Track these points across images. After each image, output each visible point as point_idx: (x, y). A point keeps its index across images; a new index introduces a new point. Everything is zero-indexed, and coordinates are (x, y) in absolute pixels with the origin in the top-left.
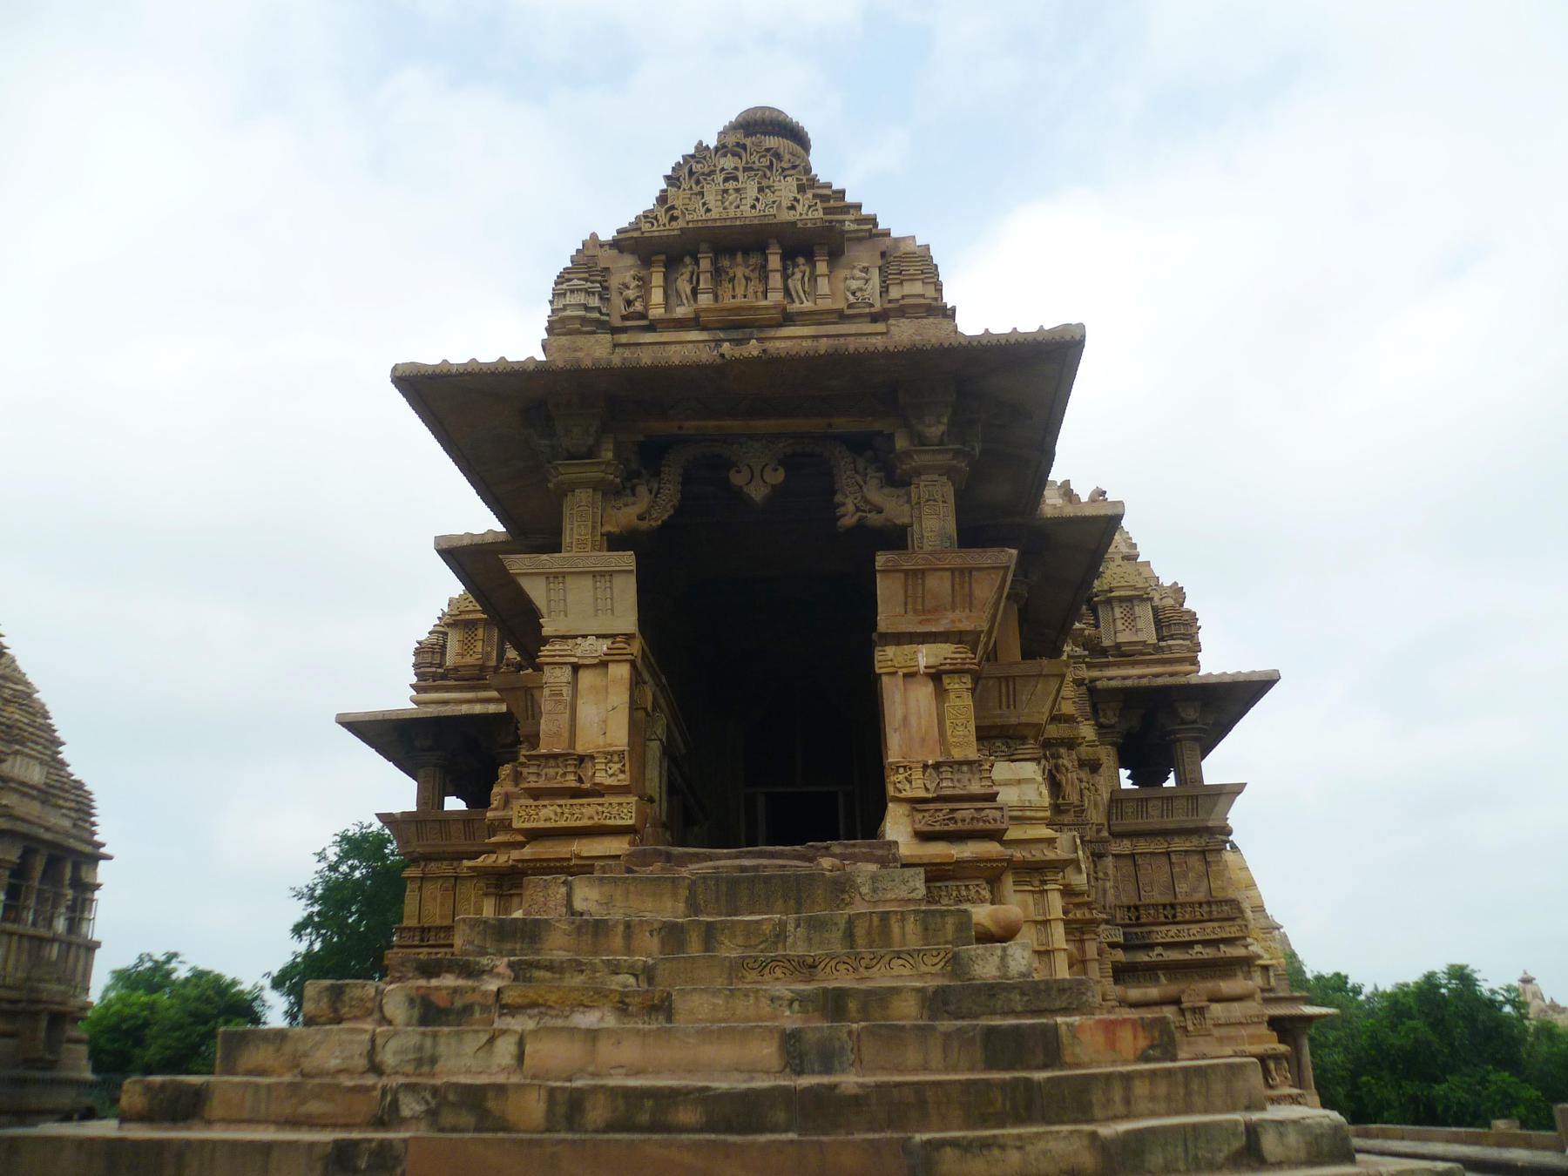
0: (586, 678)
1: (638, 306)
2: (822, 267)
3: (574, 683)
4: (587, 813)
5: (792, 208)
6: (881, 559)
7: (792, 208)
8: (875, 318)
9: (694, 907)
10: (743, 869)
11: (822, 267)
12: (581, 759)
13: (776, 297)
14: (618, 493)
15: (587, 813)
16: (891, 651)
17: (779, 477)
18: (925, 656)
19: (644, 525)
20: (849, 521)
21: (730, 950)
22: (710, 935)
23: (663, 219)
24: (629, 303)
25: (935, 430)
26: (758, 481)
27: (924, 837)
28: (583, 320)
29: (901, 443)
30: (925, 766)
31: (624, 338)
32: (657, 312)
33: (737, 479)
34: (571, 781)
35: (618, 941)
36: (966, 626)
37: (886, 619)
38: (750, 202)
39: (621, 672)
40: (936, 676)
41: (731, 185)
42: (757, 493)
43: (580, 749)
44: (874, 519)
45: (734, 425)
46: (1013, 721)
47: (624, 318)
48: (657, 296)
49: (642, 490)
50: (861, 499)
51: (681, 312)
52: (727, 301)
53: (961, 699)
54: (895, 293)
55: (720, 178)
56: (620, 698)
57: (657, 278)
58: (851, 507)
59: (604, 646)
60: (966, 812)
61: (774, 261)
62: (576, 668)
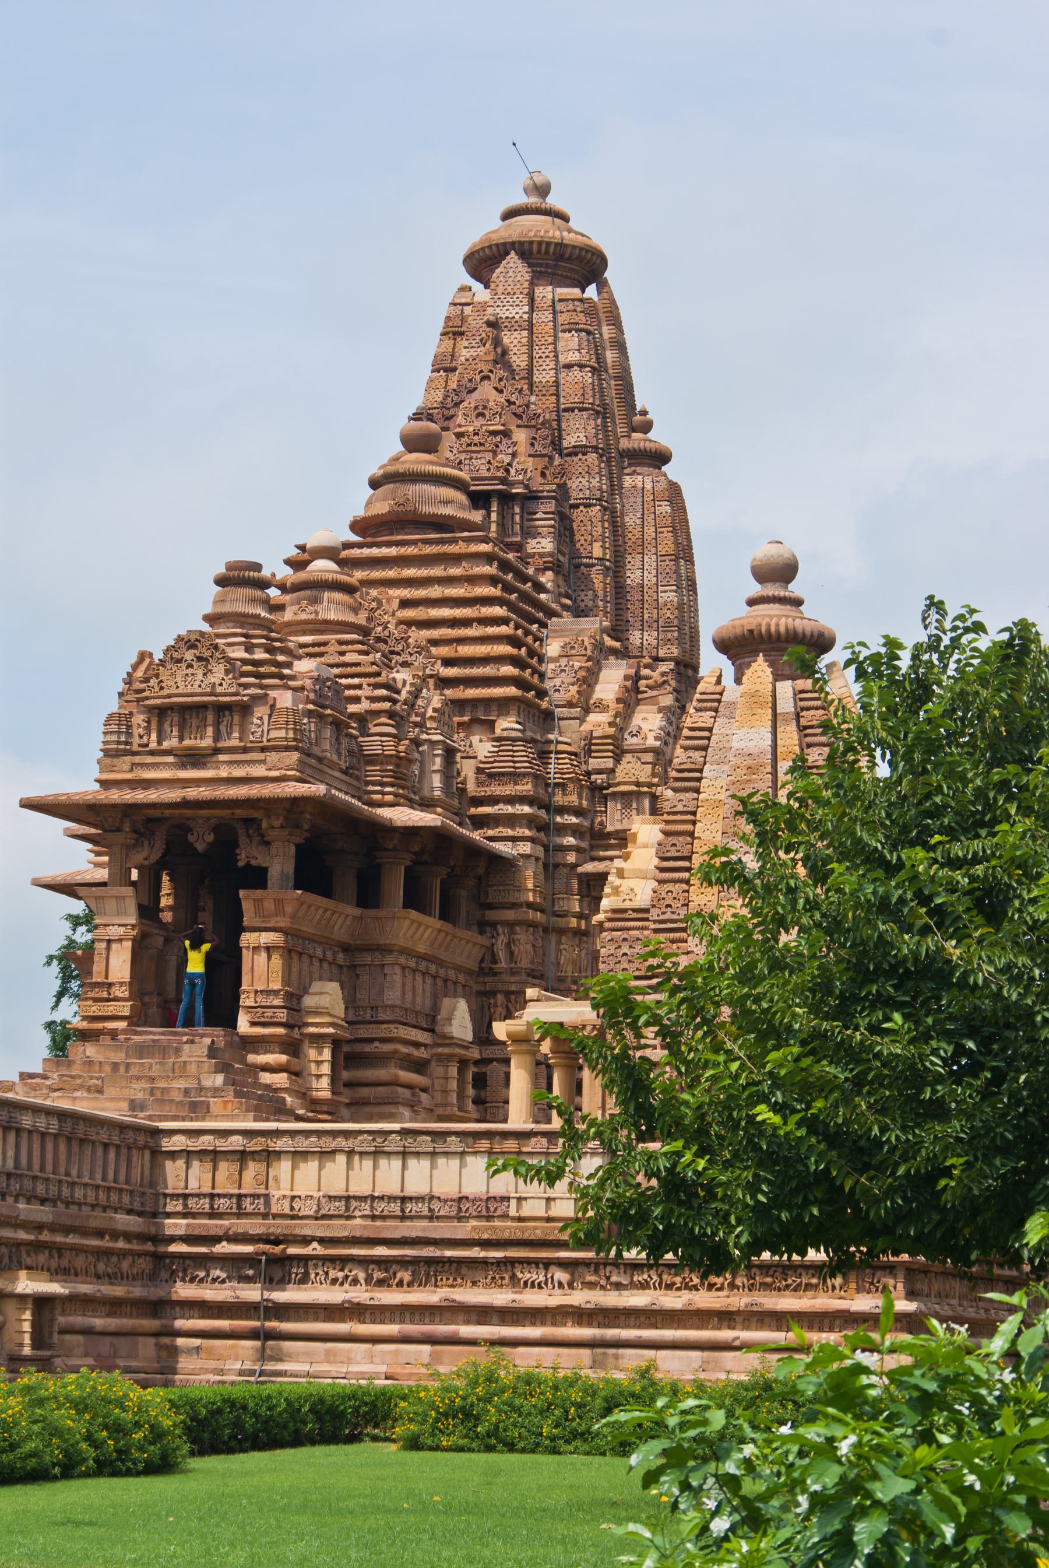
0: (114, 946)
1: (145, 739)
2: (236, 719)
3: (108, 949)
4: (111, 1009)
5: (221, 685)
6: (242, 893)
7: (221, 685)
8: (263, 749)
9: (127, 1056)
10: (154, 1041)
11: (236, 719)
12: (110, 985)
13: (207, 742)
14: (134, 846)
15: (111, 1009)
16: (248, 934)
17: (210, 838)
18: (266, 938)
19: (146, 863)
20: (241, 864)
21: (134, 1071)
22: (128, 1066)
23: (157, 689)
24: (141, 737)
25: (277, 823)
26: (202, 840)
27: (253, 1024)
28: (117, 750)
29: (264, 825)
30: (256, 992)
31: (137, 759)
32: (153, 745)
33: (191, 838)
34: (105, 995)
35: (97, 1068)
36: (282, 925)
37: (246, 922)
38: (198, 683)
39: (128, 944)
40: (268, 949)
41: (190, 671)
42: (200, 847)
43: (110, 980)
44: (253, 862)
45: (188, 812)
46: (382, 942)
47: (140, 745)
48: (154, 736)
49: (146, 843)
50: (247, 854)
51: (166, 745)
52: (187, 742)
53: (277, 961)
54: (274, 734)
55: (184, 665)
56: (127, 956)
57: (154, 725)
58: (243, 856)
59: (122, 929)
60: (269, 1013)
61: (210, 718)
62: (109, 941)
